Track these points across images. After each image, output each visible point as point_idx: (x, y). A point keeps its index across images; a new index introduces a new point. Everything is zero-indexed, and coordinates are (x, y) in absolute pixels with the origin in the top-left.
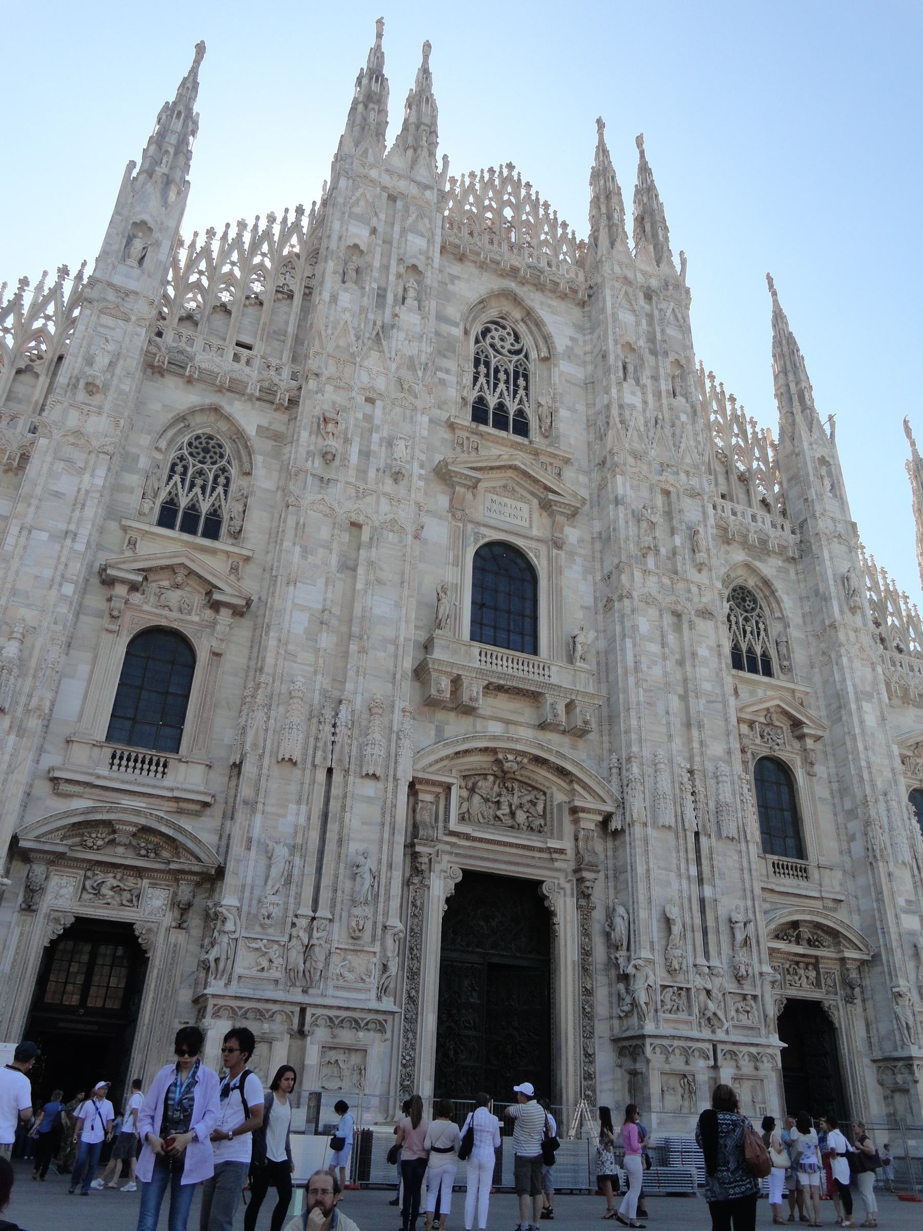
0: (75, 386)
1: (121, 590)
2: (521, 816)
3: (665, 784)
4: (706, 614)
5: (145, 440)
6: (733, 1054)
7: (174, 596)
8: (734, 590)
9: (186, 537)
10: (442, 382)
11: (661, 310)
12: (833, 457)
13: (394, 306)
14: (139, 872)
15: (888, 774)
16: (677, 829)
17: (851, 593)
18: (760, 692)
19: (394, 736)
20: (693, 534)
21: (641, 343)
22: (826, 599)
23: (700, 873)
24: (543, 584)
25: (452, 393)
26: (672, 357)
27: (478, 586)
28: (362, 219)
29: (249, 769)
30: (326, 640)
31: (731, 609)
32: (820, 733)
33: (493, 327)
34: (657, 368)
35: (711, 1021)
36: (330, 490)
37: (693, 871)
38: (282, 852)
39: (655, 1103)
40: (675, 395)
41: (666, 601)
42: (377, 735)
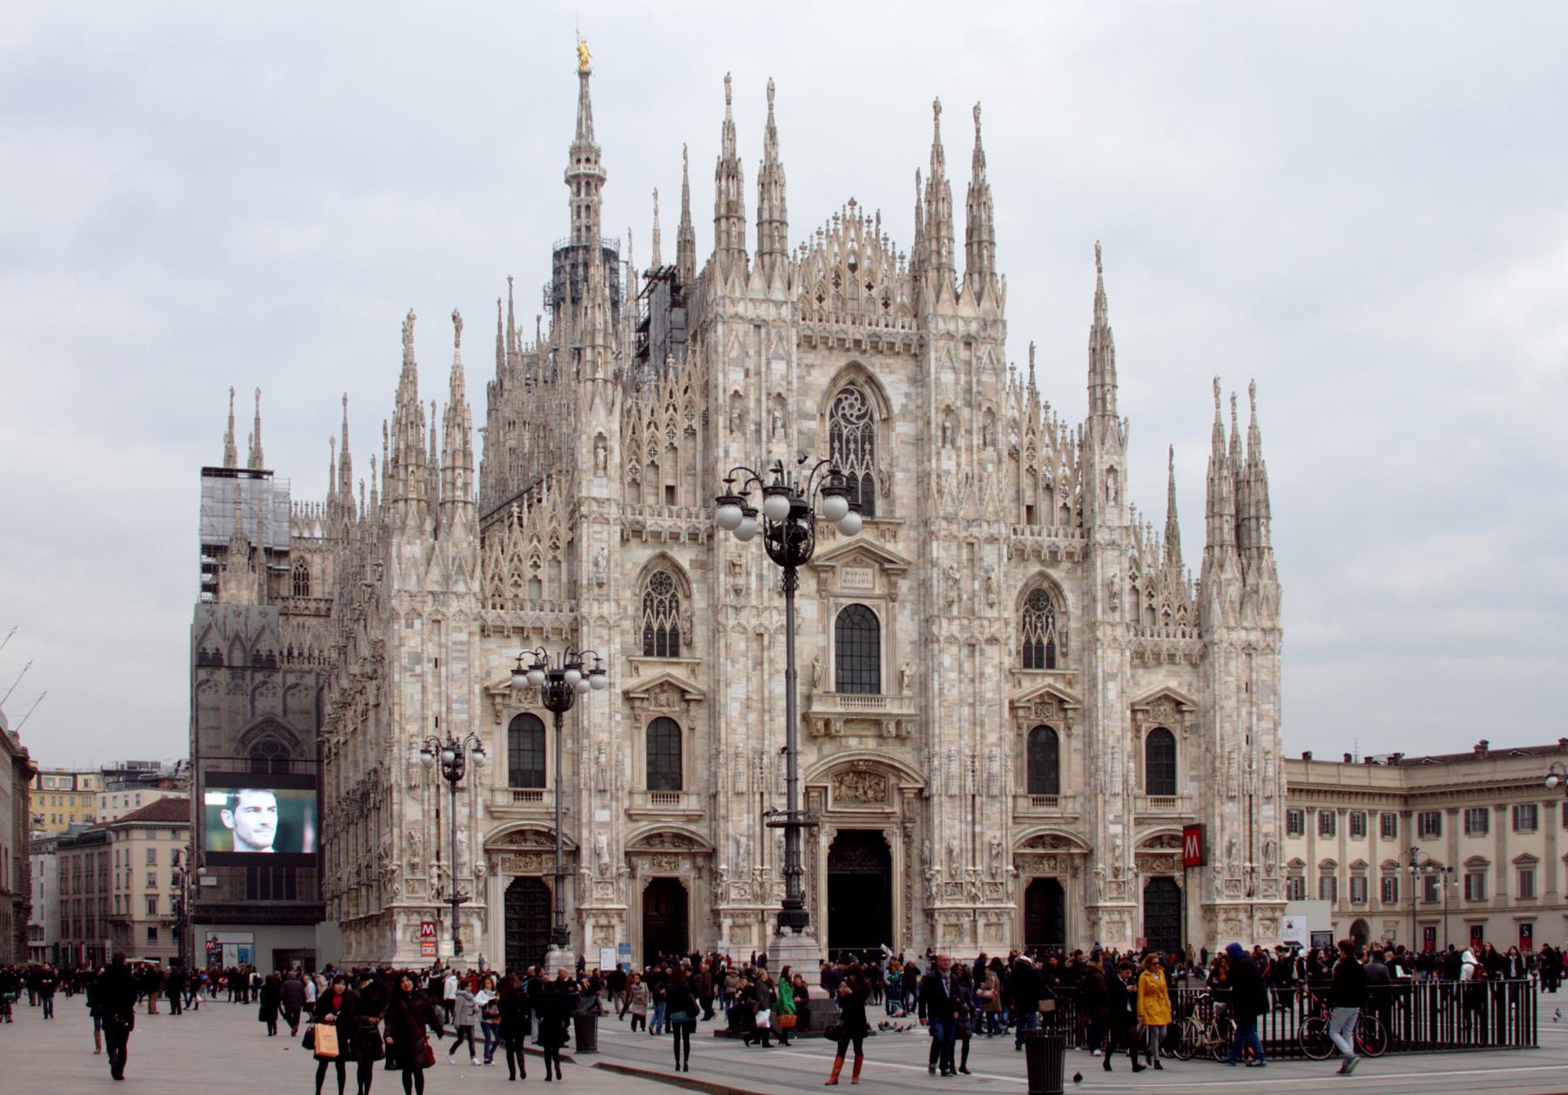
1: (638, 703)
2: (870, 794)
3: (955, 768)
4: (993, 640)
5: (628, 593)
7: (663, 698)
11: (979, 358)
12: (1120, 464)
13: (769, 441)
14: (677, 854)
15: (1118, 732)
16: (962, 796)
17: (1113, 595)
18: (1039, 679)
21: (959, 403)
22: (1094, 600)
24: (883, 631)
26: (984, 409)
27: (840, 642)
28: (739, 362)
29: (722, 799)
30: (752, 717)
33: (843, 396)
34: (971, 421)
35: (974, 898)
36: (744, 614)
37: (970, 818)
38: (744, 840)
39: (939, 939)
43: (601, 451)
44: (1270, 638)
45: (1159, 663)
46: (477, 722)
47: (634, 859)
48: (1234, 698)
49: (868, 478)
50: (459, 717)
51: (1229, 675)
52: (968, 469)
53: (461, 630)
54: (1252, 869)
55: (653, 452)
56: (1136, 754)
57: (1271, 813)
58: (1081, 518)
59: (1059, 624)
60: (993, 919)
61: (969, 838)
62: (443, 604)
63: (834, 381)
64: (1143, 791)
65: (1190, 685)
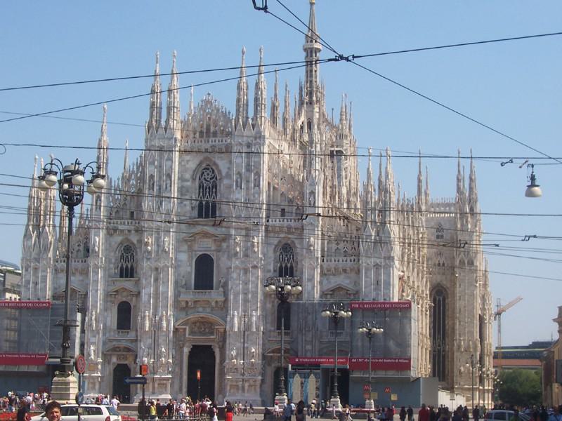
1: (113, 296)
2: (207, 330)
5: (112, 254)
7: (125, 294)
9: (124, 279)
10: (185, 205)
17: (311, 245)
19: (168, 322)
21: (243, 170)
23: (244, 342)
25: (188, 208)
28: (152, 163)
35: (243, 374)
37: (242, 340)
40: (255, 186)
42: (164, 324)
43: (99, 202)
45: (341, 274)
47: (109, 357)
58: (301, 216)
59: (295, 258)
60: (252, 383)
62: (39, 262)
63: (200, 164)
65: (355, 282)
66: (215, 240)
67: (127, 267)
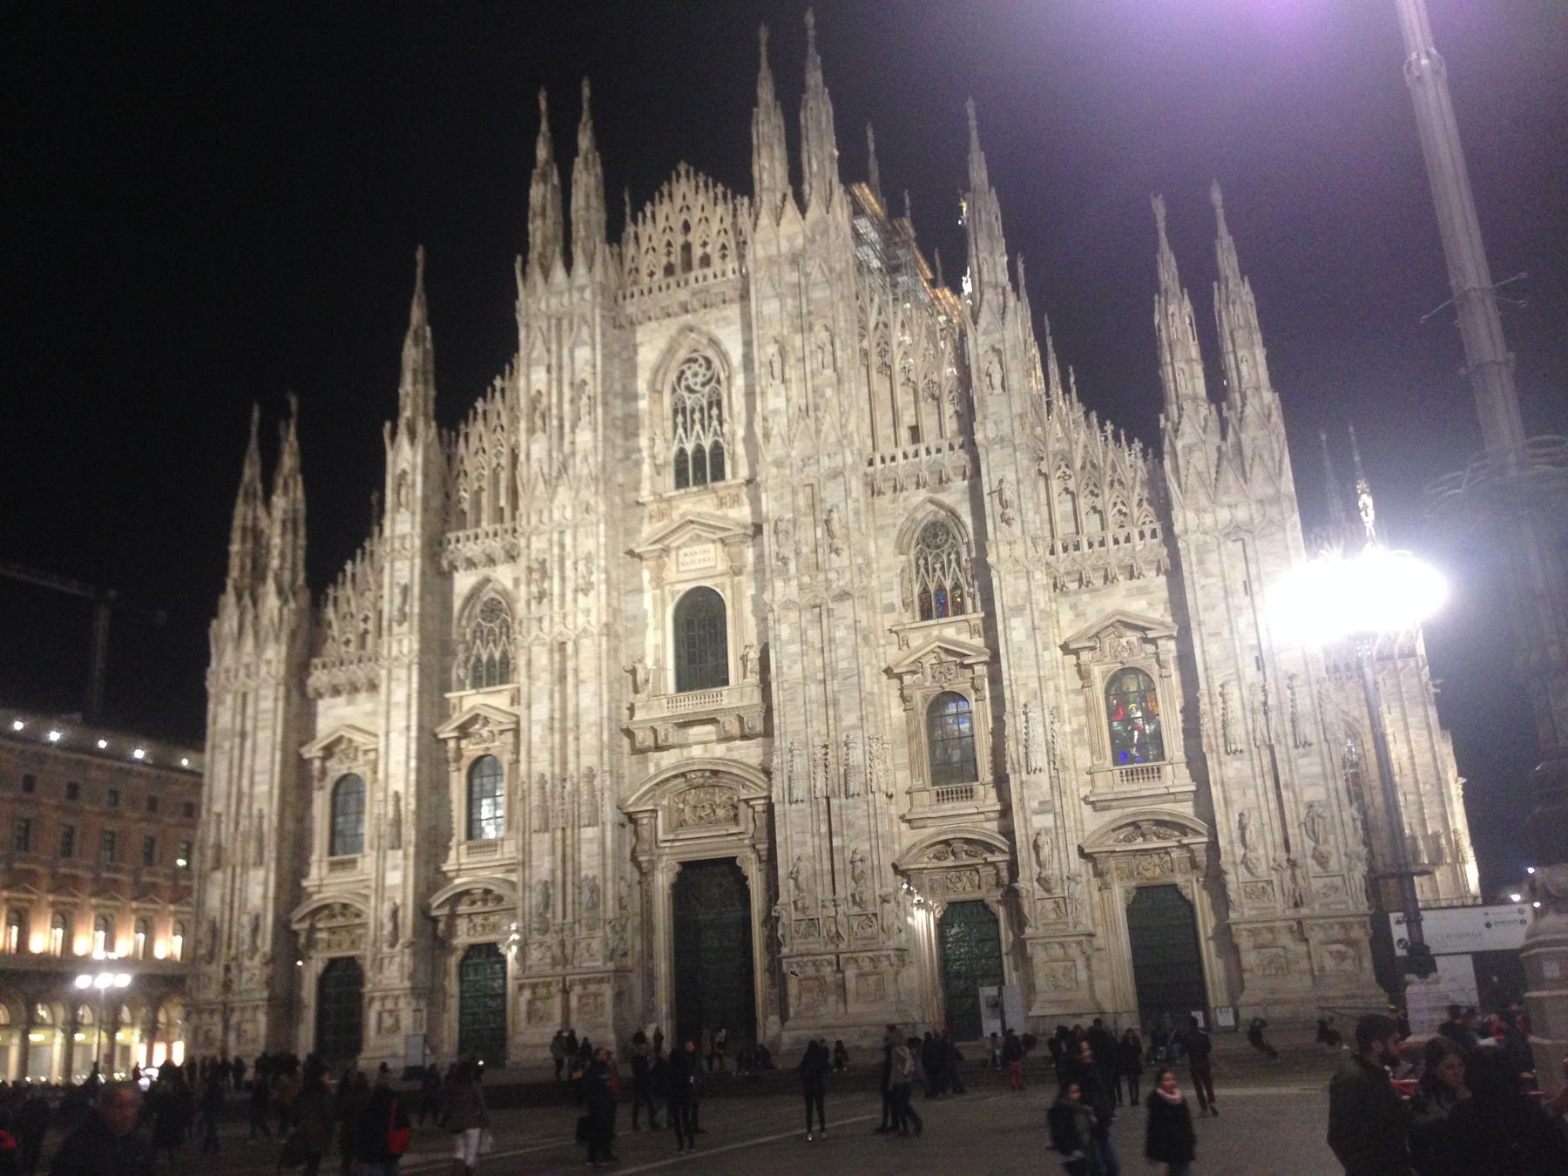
0: (390, 626)
2: (721, 813)
3: (800, 764)
4: (844, 596)
6: (856, 960)
8: (925, 530)
11: (807, 275)
15: (1034, 684)
18: (935, 632)
20: (827, 522)
21: (785, 332)
24: (729, 612)
25: (646, 469)
28: (538, 362)
31: (921, 551)
32: (985, 658)
33: (685, 367)
37: (824, 829)
39: (792, 1000)
41: (807, 598)
44: (1273, 512)
46: (276, 792)
48: (1223, 606)
49: (717, 447)
50: (262, 789)
51: (1208, 575)
52: (803, 402)
53: (266, 697)
54: (1293, 864)
55: (480, 477)
56: (1089, 709)
57: (1317, 769)
60: (867, 966)
61: (826, 855)
63: (670, 351)
64: (1108, 763)
66: (722, 540)
67: (491, 658)
